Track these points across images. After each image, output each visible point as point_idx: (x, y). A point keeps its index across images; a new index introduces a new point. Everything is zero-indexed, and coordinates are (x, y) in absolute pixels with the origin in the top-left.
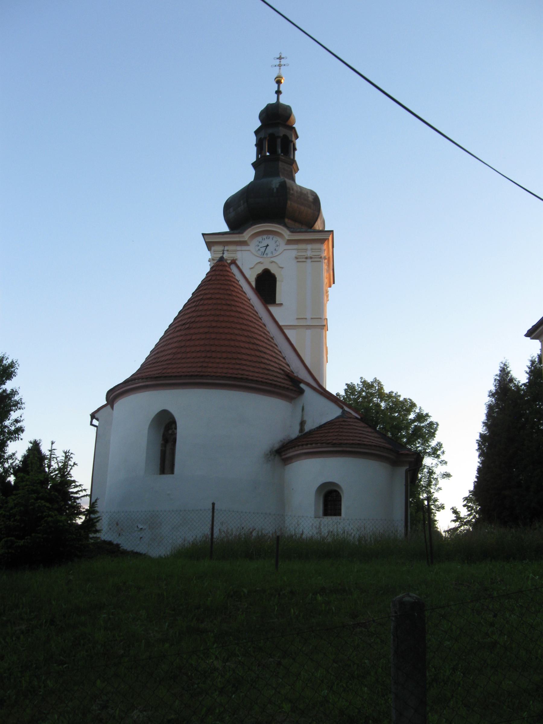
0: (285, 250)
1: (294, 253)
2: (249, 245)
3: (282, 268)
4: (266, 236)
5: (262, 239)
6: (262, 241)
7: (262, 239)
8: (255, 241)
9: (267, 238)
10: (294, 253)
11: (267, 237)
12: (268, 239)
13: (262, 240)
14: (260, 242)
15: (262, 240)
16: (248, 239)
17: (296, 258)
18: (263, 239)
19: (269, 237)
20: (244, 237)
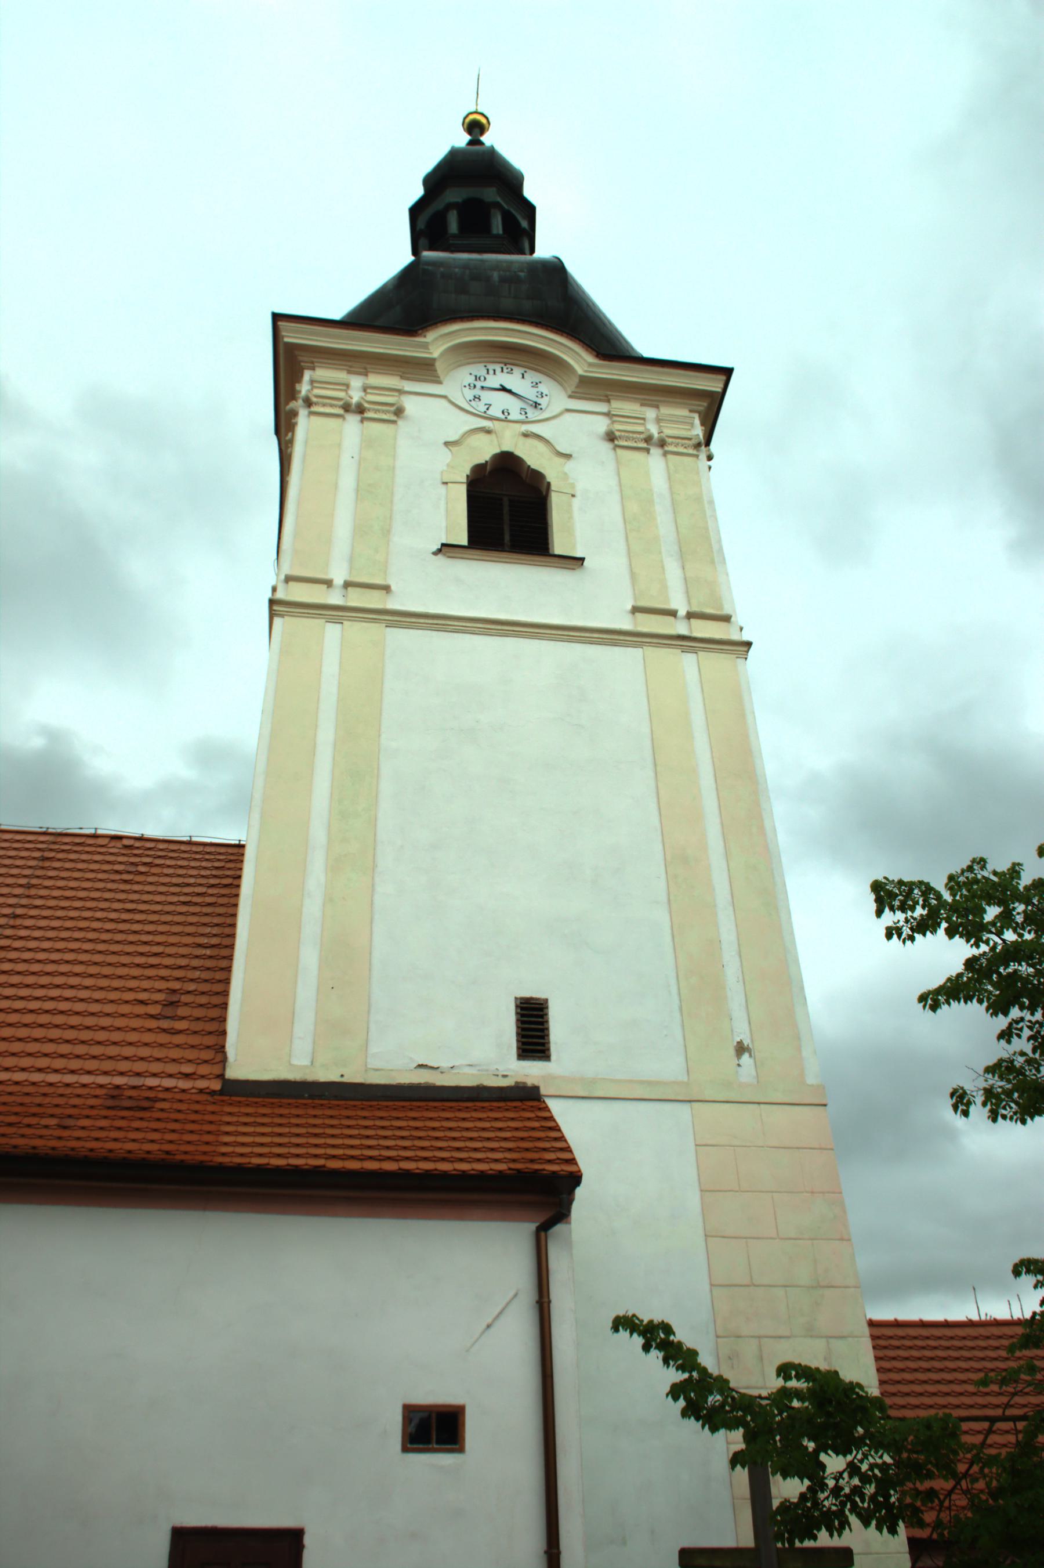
0: (568, 410)
1: (602, 425)
2: (440, 383)
3: (568, 456)
4: (503, 365)
5: (488, 370)
6: (487, 376)
7: (488, 370)
8: (465, 375)
9: (502, 371)
10: (602, 425)
11: (502, 368)
12: (508, 373)
13: (488, 373)
14: (477, 378)
15: (488, 373)
16: (442, 355)
17: (611, 437)
18: (491, 372)
19: (512, 370)
20: (425, 346)
